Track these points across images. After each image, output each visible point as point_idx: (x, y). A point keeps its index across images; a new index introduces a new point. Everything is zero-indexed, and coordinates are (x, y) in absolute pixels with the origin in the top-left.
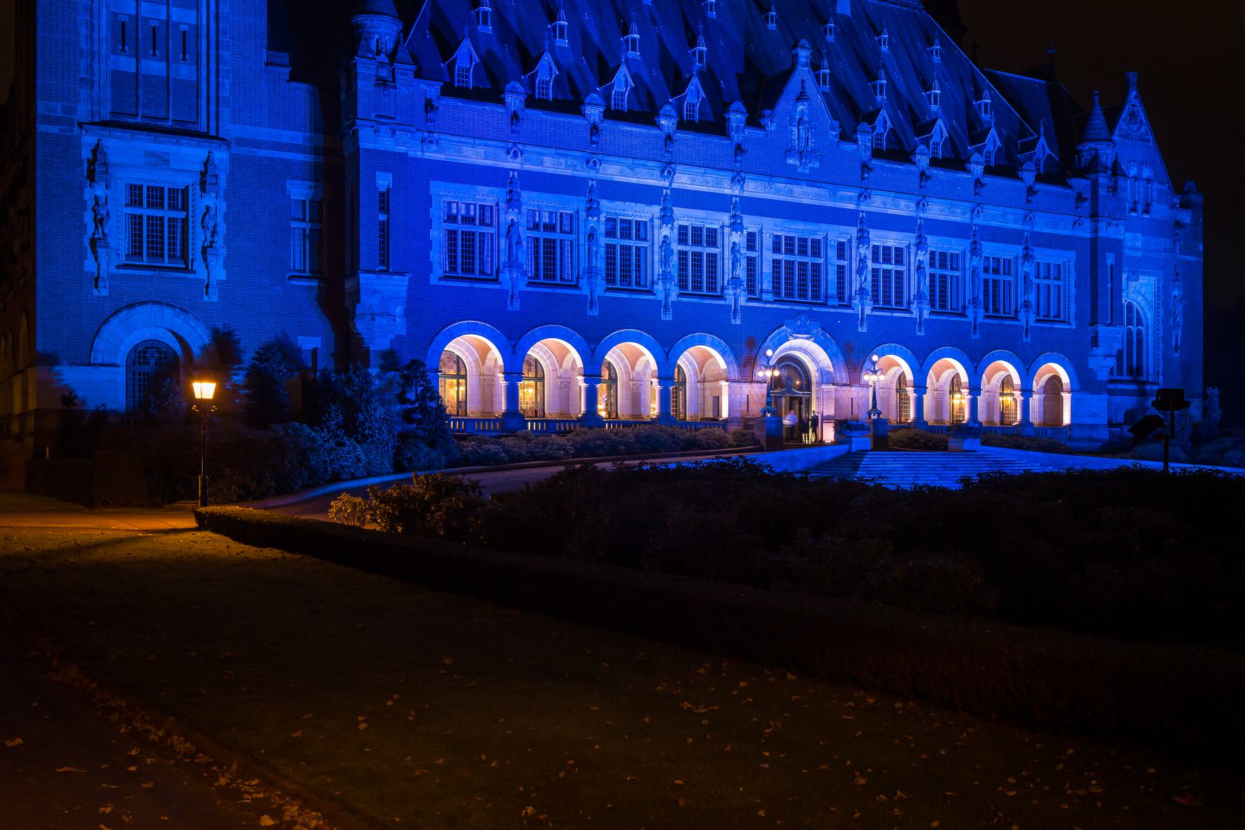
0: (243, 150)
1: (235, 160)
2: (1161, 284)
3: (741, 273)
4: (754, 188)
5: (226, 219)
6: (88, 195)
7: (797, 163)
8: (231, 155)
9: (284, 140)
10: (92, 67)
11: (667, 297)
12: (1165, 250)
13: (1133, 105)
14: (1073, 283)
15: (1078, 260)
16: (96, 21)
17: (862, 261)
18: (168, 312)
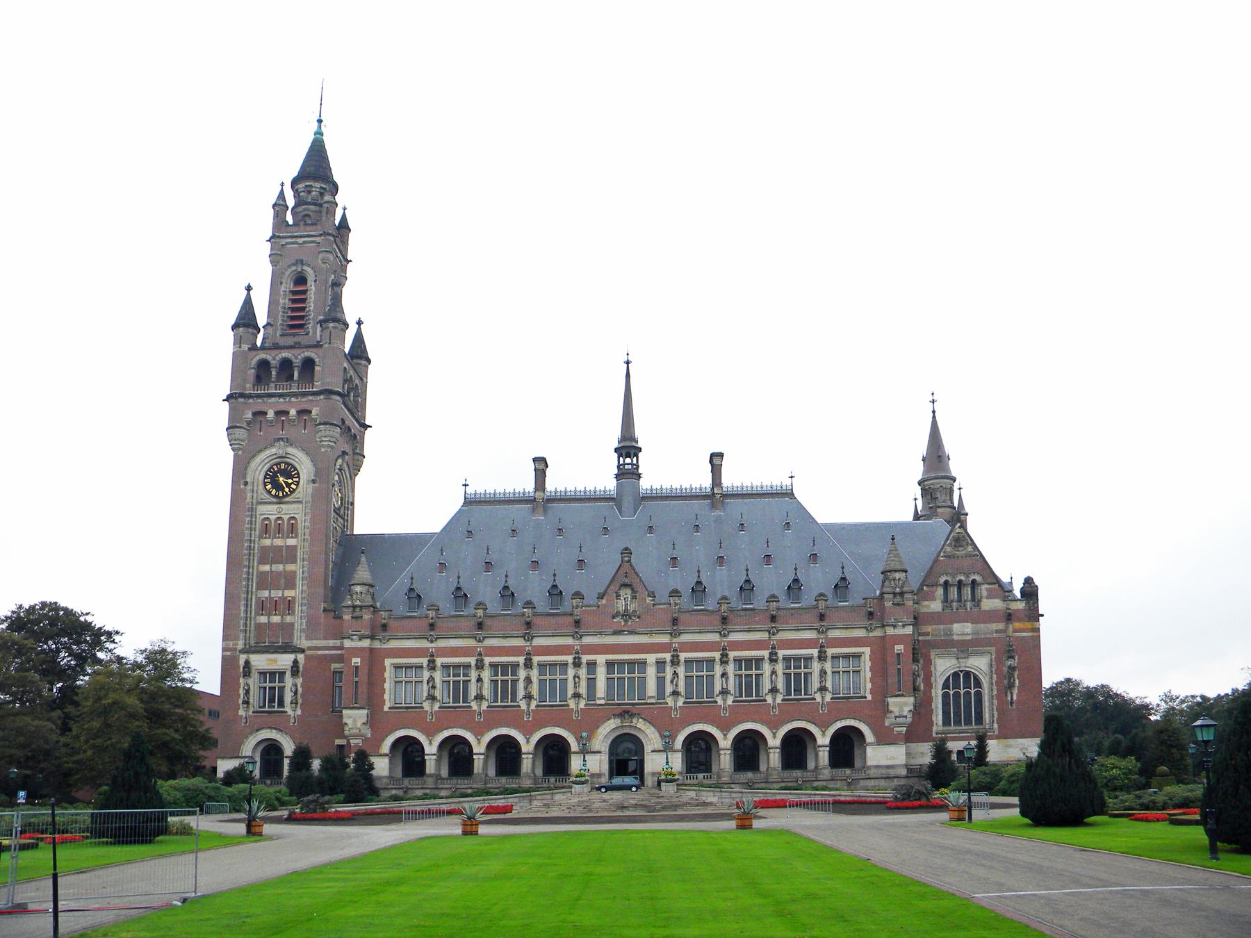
0: (312, 652)
1: (307, 658)
2: (993, 657)
3: (583, 690)
4: (587, 640)
5: (302, 686)
6: (241, 680)
7: (622, 620)
8: (305, 655)
9: (331, 645)
10: (246, 624)
11: (528, 708)
12: (997, 632)
13: (959, 533)
14: (868, 669)
15: (872, 651)
16: (249, 603)
17: (675, 674)
18: (274, 731)
